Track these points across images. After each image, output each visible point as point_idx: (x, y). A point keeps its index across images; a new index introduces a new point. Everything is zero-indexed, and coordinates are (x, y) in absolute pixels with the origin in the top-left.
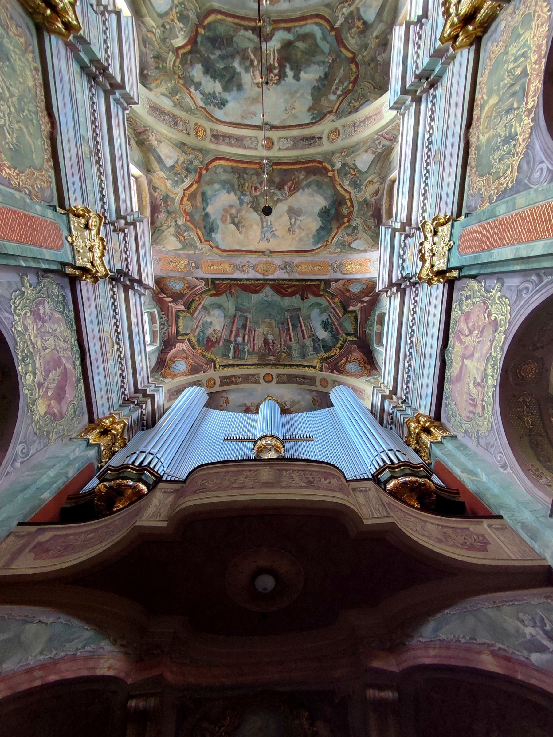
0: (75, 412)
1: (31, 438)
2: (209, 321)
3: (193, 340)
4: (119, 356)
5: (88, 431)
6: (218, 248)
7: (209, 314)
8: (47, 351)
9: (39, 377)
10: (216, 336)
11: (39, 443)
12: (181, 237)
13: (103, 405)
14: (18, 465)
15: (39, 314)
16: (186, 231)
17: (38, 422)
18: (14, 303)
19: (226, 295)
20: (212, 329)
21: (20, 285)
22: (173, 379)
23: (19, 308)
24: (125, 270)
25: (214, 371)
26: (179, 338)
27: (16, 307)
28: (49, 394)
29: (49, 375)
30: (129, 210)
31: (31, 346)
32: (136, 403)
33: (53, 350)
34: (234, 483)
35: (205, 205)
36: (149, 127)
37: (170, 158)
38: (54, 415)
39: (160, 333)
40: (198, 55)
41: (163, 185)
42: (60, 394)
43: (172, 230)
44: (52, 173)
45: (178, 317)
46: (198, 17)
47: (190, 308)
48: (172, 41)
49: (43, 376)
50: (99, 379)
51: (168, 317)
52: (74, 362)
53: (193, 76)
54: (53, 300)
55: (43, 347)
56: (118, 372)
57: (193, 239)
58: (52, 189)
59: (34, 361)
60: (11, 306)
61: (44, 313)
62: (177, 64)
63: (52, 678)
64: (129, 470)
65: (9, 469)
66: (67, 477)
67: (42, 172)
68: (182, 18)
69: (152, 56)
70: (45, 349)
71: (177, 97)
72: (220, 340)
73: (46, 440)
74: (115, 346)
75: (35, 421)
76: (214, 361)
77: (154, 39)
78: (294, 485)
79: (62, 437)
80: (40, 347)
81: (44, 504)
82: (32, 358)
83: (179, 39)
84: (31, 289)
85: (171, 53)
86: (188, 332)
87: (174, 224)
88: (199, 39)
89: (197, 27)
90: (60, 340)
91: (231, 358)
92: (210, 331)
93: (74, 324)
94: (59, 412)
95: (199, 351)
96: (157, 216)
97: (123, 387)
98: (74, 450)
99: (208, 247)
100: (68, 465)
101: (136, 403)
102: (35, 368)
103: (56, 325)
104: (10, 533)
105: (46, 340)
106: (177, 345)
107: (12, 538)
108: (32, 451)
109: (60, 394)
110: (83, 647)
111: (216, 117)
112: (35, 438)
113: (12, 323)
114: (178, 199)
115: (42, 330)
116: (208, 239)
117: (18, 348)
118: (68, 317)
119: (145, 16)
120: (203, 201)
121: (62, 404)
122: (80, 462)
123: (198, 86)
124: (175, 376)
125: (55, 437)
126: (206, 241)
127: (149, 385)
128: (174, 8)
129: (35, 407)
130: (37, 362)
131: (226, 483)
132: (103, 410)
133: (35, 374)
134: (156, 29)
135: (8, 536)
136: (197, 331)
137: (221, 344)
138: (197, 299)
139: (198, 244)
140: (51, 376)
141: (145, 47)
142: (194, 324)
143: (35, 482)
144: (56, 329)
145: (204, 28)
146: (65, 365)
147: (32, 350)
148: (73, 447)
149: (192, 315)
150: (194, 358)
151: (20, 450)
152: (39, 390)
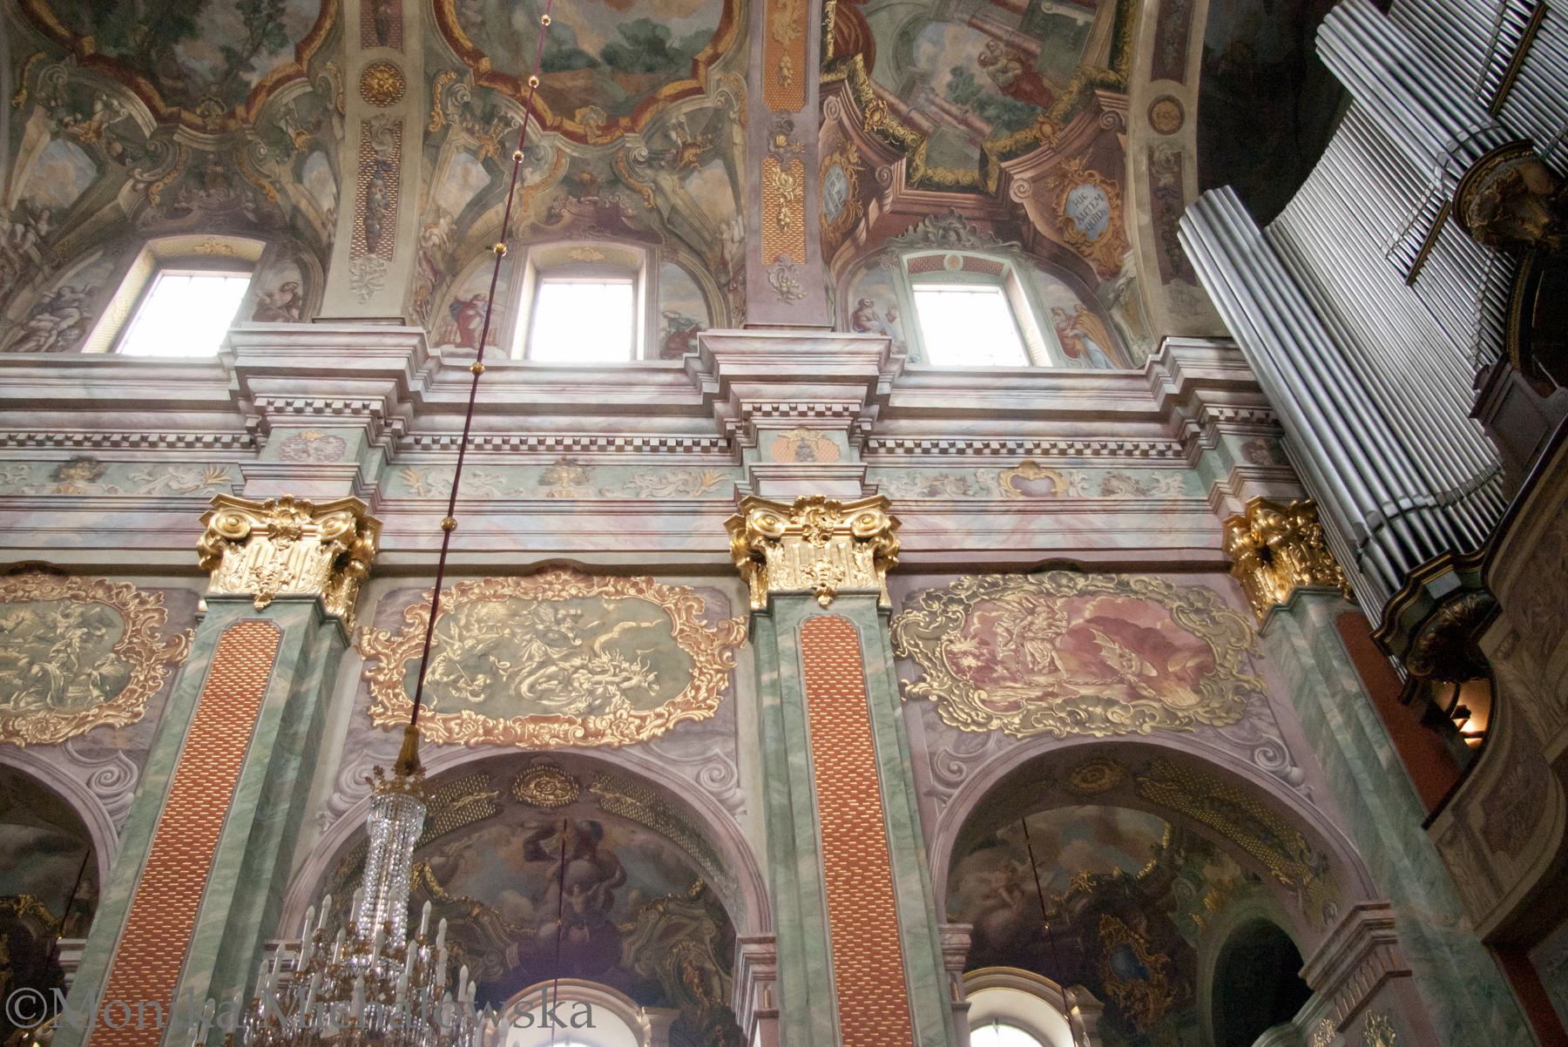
0: (1198, 611)
2: (948, 78)
3: (1005, 142)
4: (1063, 452)
5: (1249, 590)
6: (717, 37)
7: (925, 77)
8: (1059, 663)
9: (1115, 692)
10: (1003, 62)
11: (1259, 715)
12: (689, 154)
13: (1190, 531)
14: (1296, 772)
15: (979, 669)
16: (667, 137)
17: (1212, 711)
18: (966, 724)
19: (870, 14)
20: (976, 68)
21: (925, 705)
22: (1126, 247)
23: (973, 714)
24: (847, 422)
25: (1125, 91)
26: (992, 186)
27: (974, 722)
28: (1154, 673)
29: (1110, 668)
30: (683, 379)
31: (1050, 700)
32: (1194, 428)
33: (1055, 648)
35: (580, 62)
36: (417, 253)
37: (467, 172)
38: (1201, 670)
39: (973, 248)
40: (153, 54)
41: (539, 195)
42: (1153, 645)
43: (667, 181)
44: (660, 582)
45: (926, 184)
46: (60, 58)
47: (902, 142)
48: (147, 134)
49: (1112, 683)
50: (1123, 531)
51: (925, 215)
53: (213, 70)
54: (943, 628)
55: (1050, 672)
56: (1104, 460)
57: (691, 116)
58: (697, 589)
59: (1083, 698)
60: (973, 731)
61: (976, 657)
62: (199, 121)
64: (1405, 606)
65: (1301, 792)
66: (1357, 696)
67: (669, 609)
68: (80, 105)
69: (202, 193)
70: (1054, 669)
71: (291, 131)
72: (1019, 47)
73: (1255, 699)
74: (1037, 460)
75: (1210, 719)
76: (1091, 85)
77: (161, 185)
79: (1253, 656)
80: (1051, 680)
82: (1074, 702)
83: (134, 113)
84: (928, 679)
85: (176, 137)
86: (976, 155)
87: (649, 172)
88: (111, 52)
89: (83, 60)
90: (1032, 623)
91: (1091, 18)
92: (983, 78)
93: (988, 579)
94: (1193, 656)
95: (1047, 129)
96: (629, 218)
97: (1145, 454)
98: (1295, 651)
99: (715, 73)
101: (1194, 428)
102: (1097, 700)
103: (1000, 630)
105: (1034, 662)
106: (1016, 200)
108: (1273, 735)
109: (1153, 645)
111: (315, 13)
112: (1247, 725)
113: (1007, 736)
114: (570, 149)
115: (1014, 667)
116: (690, 64)
117: (1057, 731)
118: (974, 595)
119: (118, 209)
120: (568, 68)
121: (1177, 643)
122: (1330, 653)
123: (236, 61)
124: (1119, 233)
125: (1250, 676)
126: (694, 74)
127: (1153, 378)
128: (70, 130)
129: (1180, 714)
130: (1084, 691)
132: (1202, 531)
133: (1110, 703)
134: (137, 181)
135: (1441, 855)
136: (979, 124)
137: (1033, 46)
138: (877, 117)
139: (710, 102)
140: (1113, 662)
141: (189, 211)
142: (953, 131)
143: (1345, 760)
144: (1007, 630)
145: (77, 36)
146: (1089, 621)
147: (1059, 701)
148: (1286, 648)
149: (924, 135)
150: (1070, 150)
152: (1144, 697)
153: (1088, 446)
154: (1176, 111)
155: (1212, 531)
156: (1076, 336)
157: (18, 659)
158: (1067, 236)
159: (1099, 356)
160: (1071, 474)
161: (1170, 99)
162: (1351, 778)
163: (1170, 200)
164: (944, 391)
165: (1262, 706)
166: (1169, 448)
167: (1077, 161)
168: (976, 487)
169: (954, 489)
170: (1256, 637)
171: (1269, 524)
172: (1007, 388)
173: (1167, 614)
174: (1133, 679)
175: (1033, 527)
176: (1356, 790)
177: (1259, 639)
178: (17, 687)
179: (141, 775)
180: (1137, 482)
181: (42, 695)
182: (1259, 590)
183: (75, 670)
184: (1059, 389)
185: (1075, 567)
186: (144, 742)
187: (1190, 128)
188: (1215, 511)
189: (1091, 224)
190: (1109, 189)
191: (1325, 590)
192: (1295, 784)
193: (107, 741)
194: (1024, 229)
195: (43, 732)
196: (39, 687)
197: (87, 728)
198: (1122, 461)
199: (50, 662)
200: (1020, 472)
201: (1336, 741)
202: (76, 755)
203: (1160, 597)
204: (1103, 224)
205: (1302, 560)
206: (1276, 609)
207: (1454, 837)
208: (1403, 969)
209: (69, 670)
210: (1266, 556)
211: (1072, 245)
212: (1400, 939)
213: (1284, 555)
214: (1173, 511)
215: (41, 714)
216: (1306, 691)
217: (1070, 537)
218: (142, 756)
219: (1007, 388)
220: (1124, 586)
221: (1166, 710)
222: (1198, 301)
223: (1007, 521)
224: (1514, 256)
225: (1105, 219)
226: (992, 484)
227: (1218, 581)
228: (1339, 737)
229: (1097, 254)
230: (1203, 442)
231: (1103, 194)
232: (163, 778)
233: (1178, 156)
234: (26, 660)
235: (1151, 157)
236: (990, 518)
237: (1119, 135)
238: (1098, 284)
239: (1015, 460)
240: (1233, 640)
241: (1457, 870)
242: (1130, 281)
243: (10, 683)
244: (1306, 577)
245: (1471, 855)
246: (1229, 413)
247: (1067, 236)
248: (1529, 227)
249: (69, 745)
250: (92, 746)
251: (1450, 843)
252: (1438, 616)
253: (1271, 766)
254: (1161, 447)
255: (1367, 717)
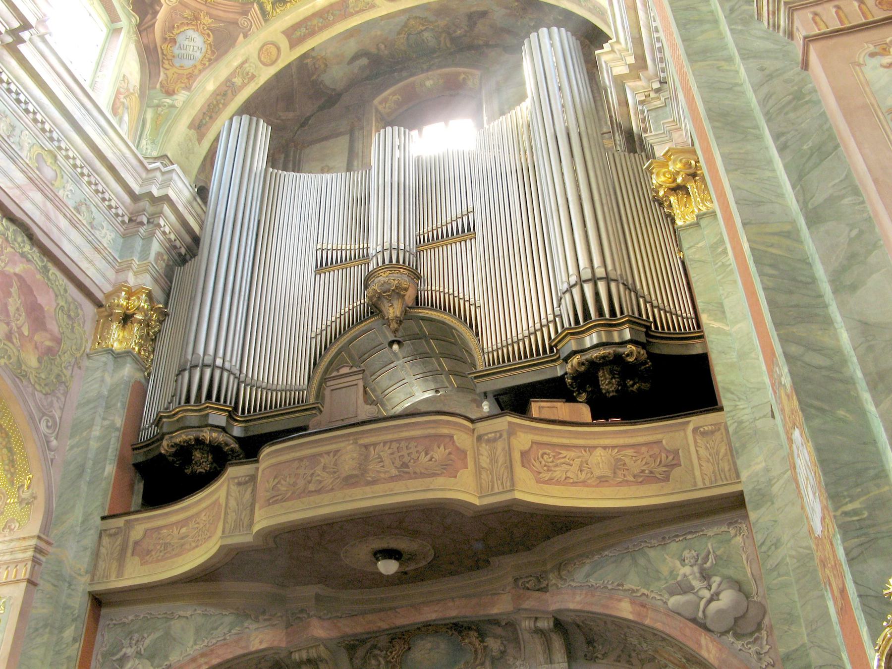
0: (69, 316)
1: (45, 404)
5: (102, 330)
11: (58, 398)
13: (98, 270)
14: (54, 443)
25: (266, 21)
29: (7, 311)
32: (145, 220)
34: (310, 482)
38: (49, 351)
50: (70, 241)
52: (23, 255)
56: (88, 191)
63: (215, 661)
66: (117, 429)
73: (62, 388)
74: (59, 157)
78: (382, 475)
79: (77, 364)
81: (113, 478)
94: (50, 340)
97: (110, 207)
100: (108, 407)
101: (145, 220)
104: (101, 534)
107: (106, 540)
110: (230, 631)
112: (49, 400)
121: (49, 326)
124: (191, 77)
127: (151, 175)
129: (24, 367)
131: (301, 483)
132: (104, 276)
135: (100, 537)
140: (12, 309)
146: (15, 274)
148: (98, 374)
150: (215, 12)
151: (45, 428)
152: (13, 343)
153: (89, 176)
154: (274, 58)
155: (108, 280)
156: (123, 103)
158: (164, 46)
159: (125, 127)
160: (68, 182)
161: (279, 49)
162: (82, 468)
163: (229, 92)
164: (51, 71)
165: (63, 394)
166: (123, 216)
167: (210, 21)
168: (17, 139)
169: (5, 128)
170: (85, 355)
171: (143, 307)
172: (83, 105)
173: (54, 304)
174: (15, 328)
175: (30, 194)
176: (80, 475)
177: (86, 357)
180: (94, 219)
182: (108, 333)
184: (106, 133)
185: (31, 237)
187: (272, 71)
188: (117, 272)
189: (183, 55)
190: (209, 52)
191: (142, 365)
192: (50, 450)
194: (149, 17)
198: (96, 200)
200: (45, 154)
201: (89, 444)
203: (58, 293)
204: (188, 64)
205: (141, 337)
206: (110, 351)
207: (115, 534)
208: (35, 581)
210: (126, 319)
211: (163, 53)
212: (44, 565)
213: (136, 328)
214: (99, 252)
216: (92, 405)
217: (43, 218)
219: (83, 105)
220: (45, 270)
221: (18, 359)
222: (193, 153)
223: (20, 178)
224: (372, 313)
225: (192, 63)
226: (26, 146)
227: (89, 308)
228: (91, 443)
229: (170, 73)
230: (142, 230)
231: (204, 50)
233: (253, 77)
235: (243, 63)
236: (13, 167)
237: (241, 35)
238: (155, 88)
239: (48, 146)
240: (74, 347)
241: (103, 550)
242: (173, 106)
244: (137, 349)
245: (118, 548)
246: (167, 230)
247: (164, 46)
248: (391, 311)
251: (110, 535)
252: (202, 431)
253: (46, 431)
254: (120, 212)
255: (114, 444)
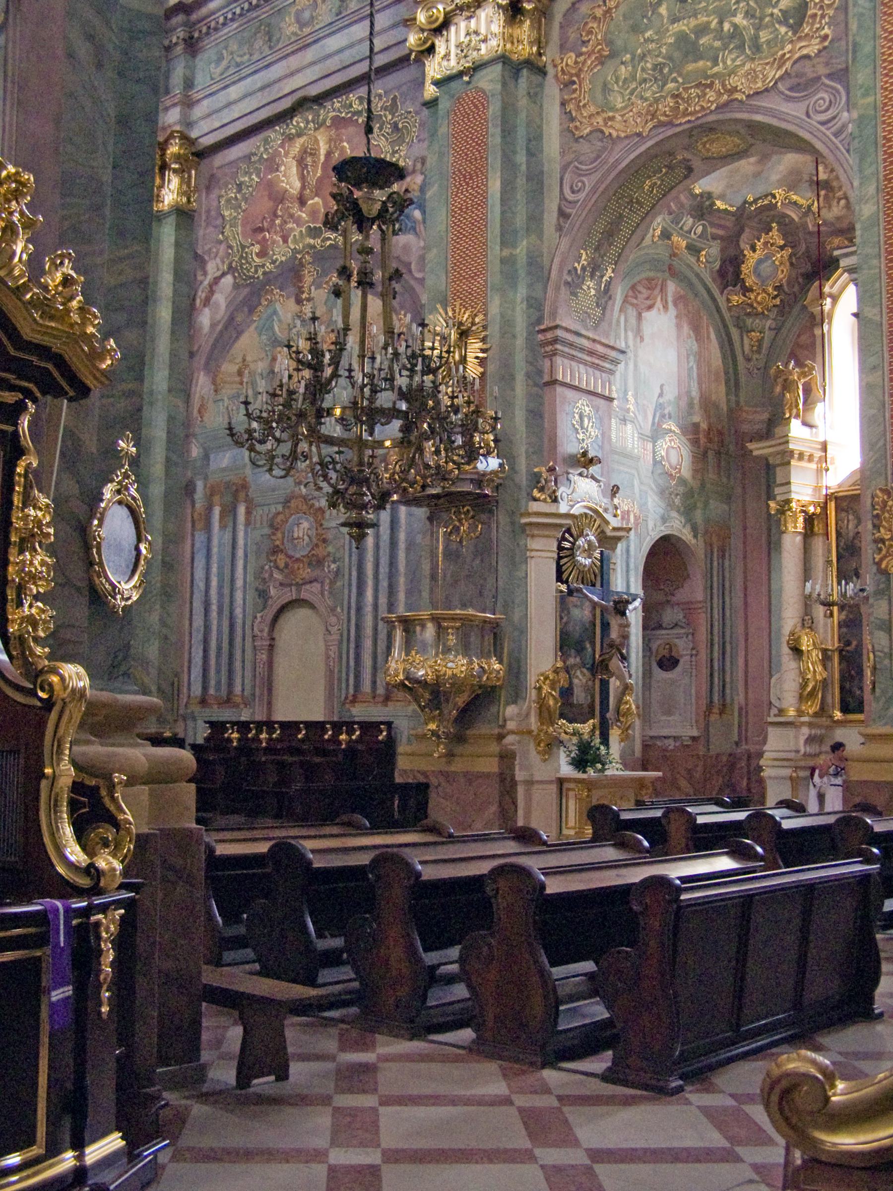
157: (709, 23)
178: (718, 49)
179: (848, 93)
181: (741, 47)
183: (758, 14)
186: (838, 64)
193: (808, 70)
195: (754, 80)
196: (736, 42)
197: (788, 65)
199: (735, 16)
202: (787, 92)
209: (753, 16)
215: (747, 66)
218: (842, 75)
232: (870, 99)
234: (716, 21)
243: (712, 47)
249: (780, 85)
250: (797, 80)
